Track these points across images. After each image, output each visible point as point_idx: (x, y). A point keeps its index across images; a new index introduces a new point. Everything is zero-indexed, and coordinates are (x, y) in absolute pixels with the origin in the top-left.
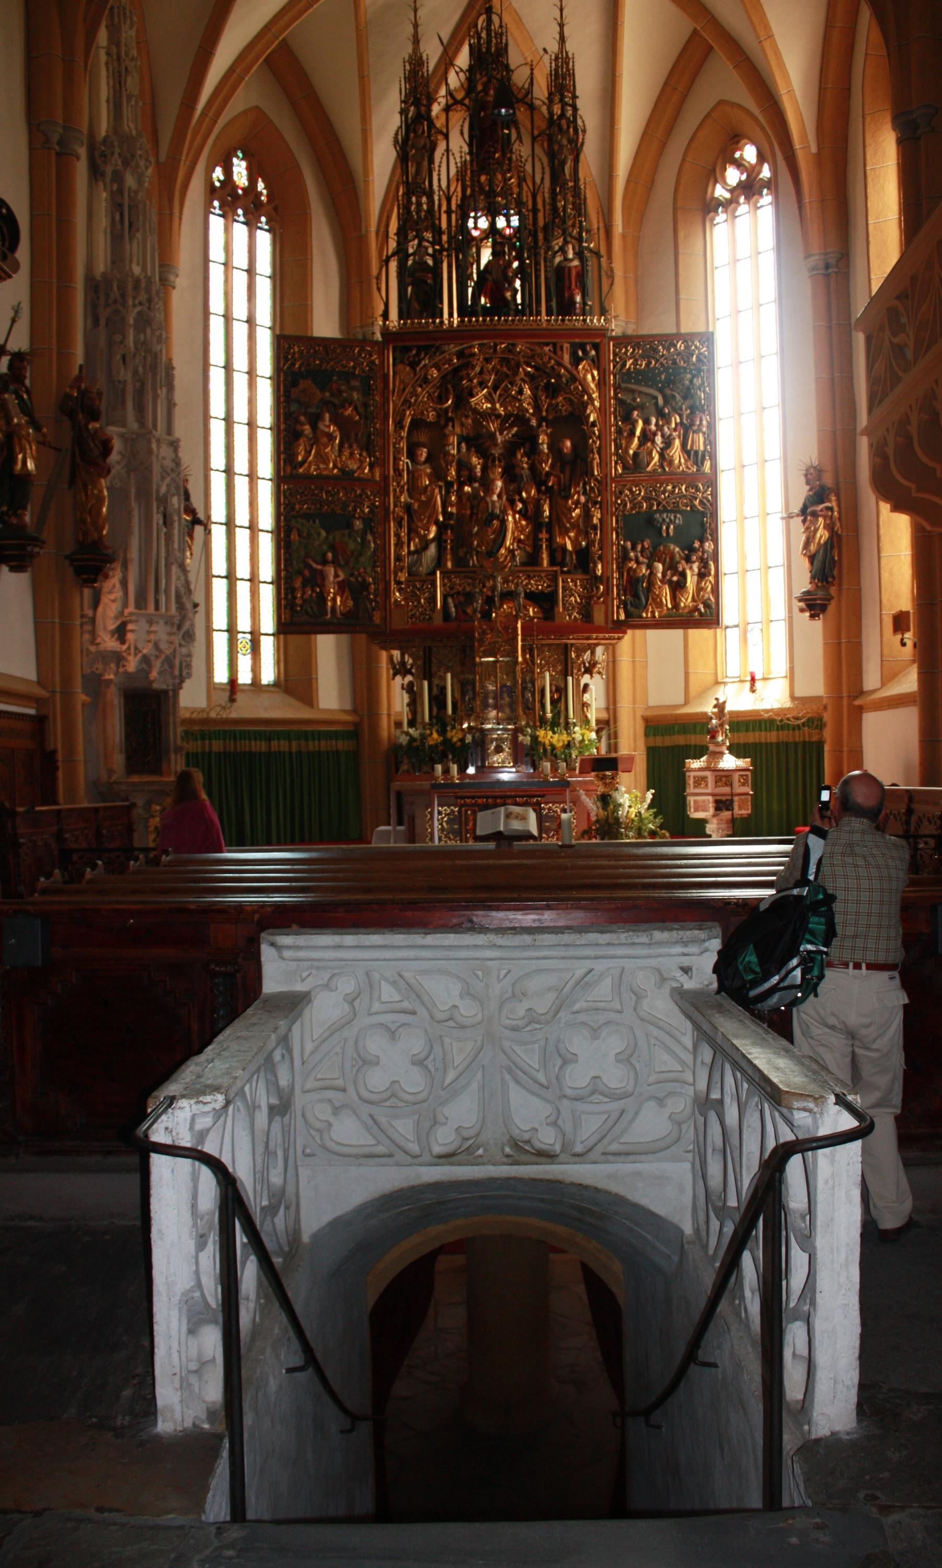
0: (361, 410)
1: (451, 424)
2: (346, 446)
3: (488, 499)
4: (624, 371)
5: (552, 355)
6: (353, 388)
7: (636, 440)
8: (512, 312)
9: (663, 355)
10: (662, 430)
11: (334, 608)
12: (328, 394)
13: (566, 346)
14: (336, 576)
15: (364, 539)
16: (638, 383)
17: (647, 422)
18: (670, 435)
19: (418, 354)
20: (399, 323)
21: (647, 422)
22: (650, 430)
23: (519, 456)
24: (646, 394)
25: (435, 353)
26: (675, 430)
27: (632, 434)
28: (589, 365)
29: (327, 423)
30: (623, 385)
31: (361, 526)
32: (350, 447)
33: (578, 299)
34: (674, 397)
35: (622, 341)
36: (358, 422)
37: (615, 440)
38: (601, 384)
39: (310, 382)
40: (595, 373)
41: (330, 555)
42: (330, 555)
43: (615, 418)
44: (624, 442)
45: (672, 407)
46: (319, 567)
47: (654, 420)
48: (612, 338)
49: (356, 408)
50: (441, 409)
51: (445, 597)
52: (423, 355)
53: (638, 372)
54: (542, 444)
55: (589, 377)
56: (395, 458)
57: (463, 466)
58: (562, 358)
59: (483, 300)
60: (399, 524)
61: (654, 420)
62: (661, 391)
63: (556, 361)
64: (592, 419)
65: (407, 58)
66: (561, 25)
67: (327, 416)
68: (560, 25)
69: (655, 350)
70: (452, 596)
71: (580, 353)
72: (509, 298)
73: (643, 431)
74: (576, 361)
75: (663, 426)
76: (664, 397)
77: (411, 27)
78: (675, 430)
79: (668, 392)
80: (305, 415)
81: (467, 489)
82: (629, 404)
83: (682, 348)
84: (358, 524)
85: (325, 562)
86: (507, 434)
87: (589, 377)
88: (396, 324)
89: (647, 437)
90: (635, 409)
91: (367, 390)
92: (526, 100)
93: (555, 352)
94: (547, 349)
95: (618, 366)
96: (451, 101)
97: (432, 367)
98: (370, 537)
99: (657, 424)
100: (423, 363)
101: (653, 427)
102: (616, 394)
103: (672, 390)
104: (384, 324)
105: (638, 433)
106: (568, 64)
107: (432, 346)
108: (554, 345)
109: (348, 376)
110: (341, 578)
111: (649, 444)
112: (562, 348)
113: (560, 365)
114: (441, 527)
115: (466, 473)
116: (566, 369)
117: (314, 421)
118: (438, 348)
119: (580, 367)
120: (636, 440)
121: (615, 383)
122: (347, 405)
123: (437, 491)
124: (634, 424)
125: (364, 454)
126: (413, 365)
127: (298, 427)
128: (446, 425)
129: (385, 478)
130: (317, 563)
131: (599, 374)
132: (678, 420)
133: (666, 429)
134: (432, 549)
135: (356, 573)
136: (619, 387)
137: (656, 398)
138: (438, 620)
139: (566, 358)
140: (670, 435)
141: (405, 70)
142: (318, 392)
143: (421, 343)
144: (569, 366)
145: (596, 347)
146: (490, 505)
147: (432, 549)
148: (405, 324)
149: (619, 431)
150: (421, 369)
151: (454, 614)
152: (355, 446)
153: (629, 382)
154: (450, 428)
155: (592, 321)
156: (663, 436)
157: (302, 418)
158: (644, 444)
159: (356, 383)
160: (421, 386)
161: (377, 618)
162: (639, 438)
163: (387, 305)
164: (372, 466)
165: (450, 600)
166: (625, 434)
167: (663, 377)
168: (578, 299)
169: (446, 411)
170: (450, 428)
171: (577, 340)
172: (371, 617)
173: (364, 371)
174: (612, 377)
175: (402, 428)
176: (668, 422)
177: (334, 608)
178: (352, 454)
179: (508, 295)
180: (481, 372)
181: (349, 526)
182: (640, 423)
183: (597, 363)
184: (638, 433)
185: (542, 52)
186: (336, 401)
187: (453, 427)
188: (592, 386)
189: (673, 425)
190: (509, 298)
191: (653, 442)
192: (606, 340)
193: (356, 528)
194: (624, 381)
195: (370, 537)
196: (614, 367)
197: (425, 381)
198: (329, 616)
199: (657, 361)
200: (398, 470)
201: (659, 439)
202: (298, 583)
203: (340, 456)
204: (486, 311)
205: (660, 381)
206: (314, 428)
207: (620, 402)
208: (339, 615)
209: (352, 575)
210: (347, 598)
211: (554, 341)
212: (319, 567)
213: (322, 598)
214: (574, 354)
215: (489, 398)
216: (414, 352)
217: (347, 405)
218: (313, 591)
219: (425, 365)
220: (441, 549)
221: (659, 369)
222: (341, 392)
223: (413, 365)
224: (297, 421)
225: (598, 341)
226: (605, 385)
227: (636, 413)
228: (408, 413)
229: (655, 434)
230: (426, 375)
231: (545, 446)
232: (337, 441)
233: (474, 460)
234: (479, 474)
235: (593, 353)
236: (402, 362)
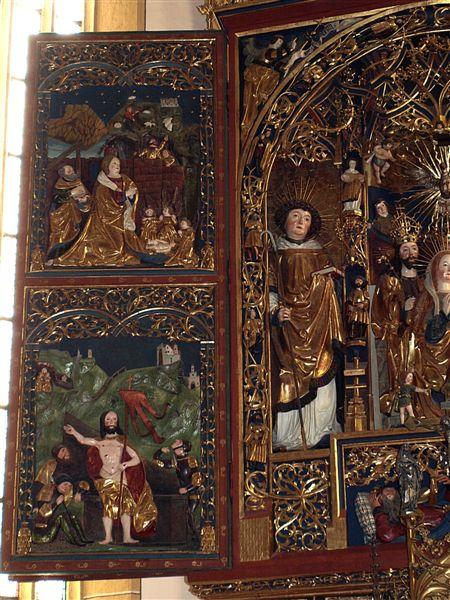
1: (353, 163)
2: (150, 212)
3: (433, 292)
6: (166, 112)
11: (117, 526)
12: (118, 125)
14: (125, 457)
15: (183, 382)
19: (285, 47)
25: (317, 40)
31: (177, 358)
39: (86, 107)
41: (111, 419)
42: (111, 419)
46: (92, 442)
49: (170, 146)
50: (332, 136)
51: (351, 494)
56: (245, 231)
57: (382, 239)
60: (257, 350)
70: (368, 489)
80: (73, 163)
81: (393, 282)
84: (171, 355)
85: (103, 432)
91: (190, 111)
98: (194, 378)
100: (295, 57)
109: (154, 93)
110: (135, 462)
114: (342, 356)
115: (391, 252)
117: (89, 173)
118: (322, 27)
123: (330, 283)
125: (185, 225)
127: (61, 186)
128: (345, 167)
129: (227, 265)
130: (86, 435)
134: (326, 397)
135: (165, 450)
138: (337, 540)
142: (100, 124)
146: (437, 303)
147: (326, 397)
150: (291, 69)
151: (372, 529)
154: (352, 170)
157: (68, 170)
159: (173, 104)
160: (293, 99)
161: (209, 538)
164: (198, 246)
165: (362, 499)
169: (343, 138)
170: (352, 170)
172: (196, 540)
175: (259, 173)
177: (117, 526)
180: (407, 62)
181: (151, 359)
186: (132, 137)
187: (359, 168)
193: (166, 361)
195: (194, 378)
197: (301, 86)
198: (109, 538)
200: (252, 249)
202: (47, 474)
206: (91, 185)
208: (128, 538)
209: (158, 454)
210: (145, 500)
212: (92, 442)
213: (94, 504)
215: (427, 107)
216: (279, 43)
218: (76, 490)
219: (300, 59)
220: (342, 397)
223: (278, 64)
224: (56, 175)
228: (269, 147)
233: (405, 226)
234: (415, 252)
236: (258, 62)
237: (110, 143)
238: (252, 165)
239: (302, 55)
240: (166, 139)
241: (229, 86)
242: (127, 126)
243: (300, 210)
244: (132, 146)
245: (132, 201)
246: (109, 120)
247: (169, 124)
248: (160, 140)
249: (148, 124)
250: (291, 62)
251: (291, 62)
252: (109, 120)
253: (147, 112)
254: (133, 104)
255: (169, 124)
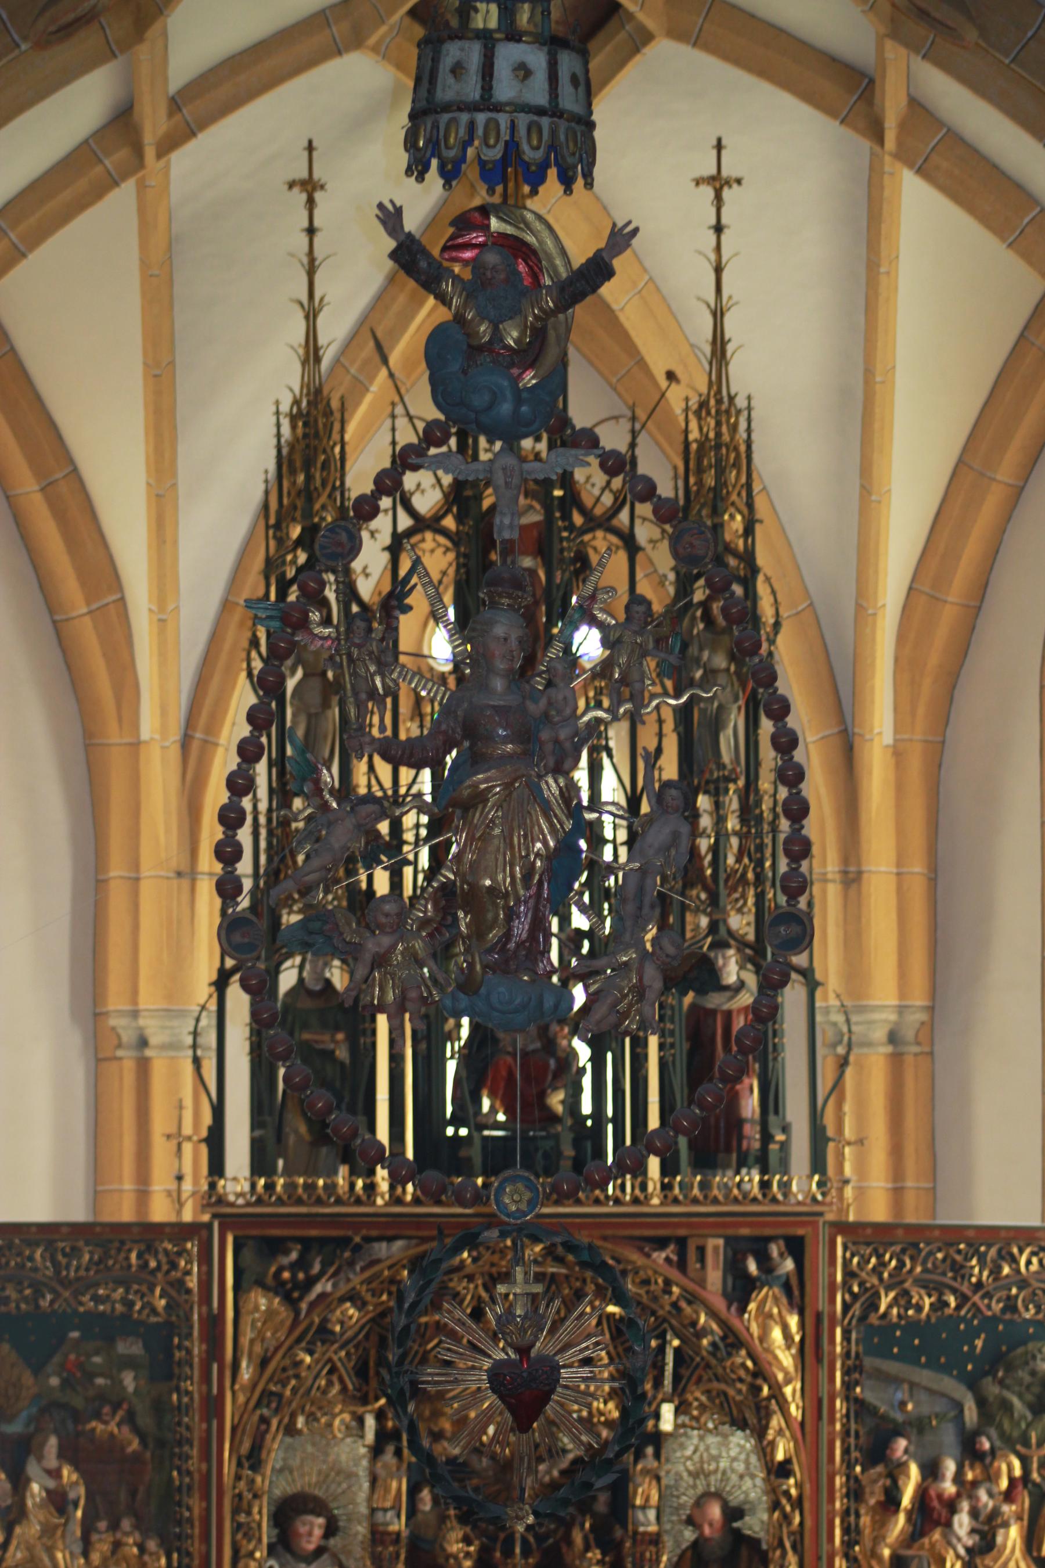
0: (145, 1420)
2: (102, 1525)
4: (873, 1319)
5: (674, 1274)
7: (902, 1518)
8: (566, 1164)
9: (979, 1285)
10: (972, 1497)
12: (54, 1381)
13: (715, 1244)
16: (910, 1357)
17: (931, 1471)
18: (995, 1513)
19: (302, 1263)
20: (253, 1186)
21: (931, 1471)
22: (940, 1496)
23: (578, 1538)
24: (931, 1392)
25: (351, 1264)
26: (1009, 1496)
27: (891, 1501)
28: (776, 1300)
29: (52, 1462)
30: (868, 1362)
32: (114, 1526)
33: (751, 1104)
34: (1006, 1407)
35: (866, 1236)
36: (136, 1457)
37: (846, 1513)
38: (811, 1351)
40: (793, 1321)
43: (846, 1451)
44: (865, 1520)
45: (1002, 1435)
47: (950, 1467)
48: (841, 1227)
49: (130, 1419)
52: (316, 1268)
53: (913, 1327)
54: (644, 1508)
55: (777, 1334)
58: (702, 1283)
59: (486, 1104)
61: (950, 1467)
62: (972, 1383)
63: (683, 1289)
64: (780, 1456)
65: (285, 407)
66: (718, 314)
67: (53, 1441)
68: (714, 314)
69: (959, 1270)
71: (752, 1267)
72: (560, 1109)
73: (922, 1496)
74: (740, 1290)
75: (975, 1484)
76: (981, 1403)
77: (300, 315)
78: (1009, 1496)
79: (992, 1389)
82: (884, 1418)
83: (1035, 1266)
86: (549, 1472)
87: (777, 1334)
88: (246, 1187)
89: (930, 1514)
90: (898, 1431)
91: (163, 1367)
92: (615, 522)
93: (682, 1265)
94: (659, 1256)
95: (857, 1309)
96: (405, 522)
97: (342, 1300)
99: (958, 1478)
100: (318, 1288)
101: (949, 1487)
102: (848, 1386)
103: (1001, 1383)
104: (212, 1186)
105: (906, 1501)
106: (734, 428)
107: (345, 1241)
108: (682, 1243)
109: (106, 1329)
111: (937, 1535)
112: (701, 1250)
113: (692, 1299)
116: (712, 1314)
119: (752, 1306)
120: (902, 1518)
121: (847, 1355)
122: (106, 1409)
124: (895, 1473)
125: (152, 1545)
126: (290, 1293)
131: (802, 1325)
132: (1018, 1472)
133: (983, 1495)
136: (858, 1368)
137: (959, 1407)
139: (714, 1276)
140: (995, 1513)
141: (279, 435)
142: (28, 1379)
143: (314, 1233)
144: (720, 1304)
145: (796, 1247)
148: (270, 1187)
149: (855, 1492)
150: (312, 1306)
152: (126, 1524)
153: (890, 1356)
155: (785, 1186)
156: (974, 1513)
158: (923, 1534)
162: (909, 1514)
163: (218, 1111)
166: (872, 1501)
167: (979, 1343)
168: (751, 1104)
171: (745, 1231)
173: (154, 1311)
174: (838, 1331)
176: (990, 1477)
178: (117, 1545)
179: (556, 1100)
182: (914, 1470)
183: (796, 1294)
184: (906, 1501)
185: (663, 383)
186: (78, 1402)
188: (787, 1359)
189: (1004, 1484)
190: (560, 1109)
191: (949, 1524)
192: (823, 1234)
194: (873, 1351)
196: (846, 1307)
197: (323, 1332)
199: (963, 1299)
201: (962, 1522)
203: (86, 1554)
204: (498, 1158)
205: (971, 1356)
207: (860, 1408)
211: (682, 1232)
214: (734, 1267)
216: (294, 1256)
217: (106, 1409)
219: (323, 1296)
221: (969, 1323)
222: (90, 1376)
225: (800, 1232)
226: (819, 1359)
227: (902, 1443)
229: (952, 1506)
230: (325, 1321)
231: (652, 1514)
232: (79, 1513)
235: (789, 1265)
236: (261, 1283)
237: (43, 1411)
238: (249, 1457)
239: (329, 1287)
240: (125, 1406)
241: (213, 1324)
242: (66, 1383)
243: (310, 1518)
244: (77, 1417)
245: (76, 1504)
246: (38, 1370)
247: (129, 1380)
248: (116, 1407)
249: (100, 1381)
250: (313, 1295)
251: (313, 1295)
252: (38, 1370)
253: (97, 1360)
254: (77, 1342)
255: (129, 1380)
